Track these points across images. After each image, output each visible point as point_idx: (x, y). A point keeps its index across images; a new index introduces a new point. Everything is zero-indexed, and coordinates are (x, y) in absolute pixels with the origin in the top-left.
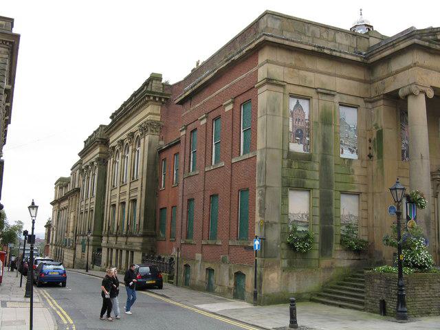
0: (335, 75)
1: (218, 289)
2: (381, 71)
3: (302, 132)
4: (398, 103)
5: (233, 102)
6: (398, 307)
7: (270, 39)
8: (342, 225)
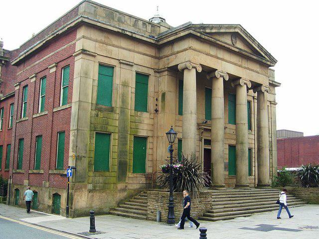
1: (41, 207)
2: (167, 51)
4: (177, 74)
5: (56, 66)
6: (168, 215)
7: (86, 20)
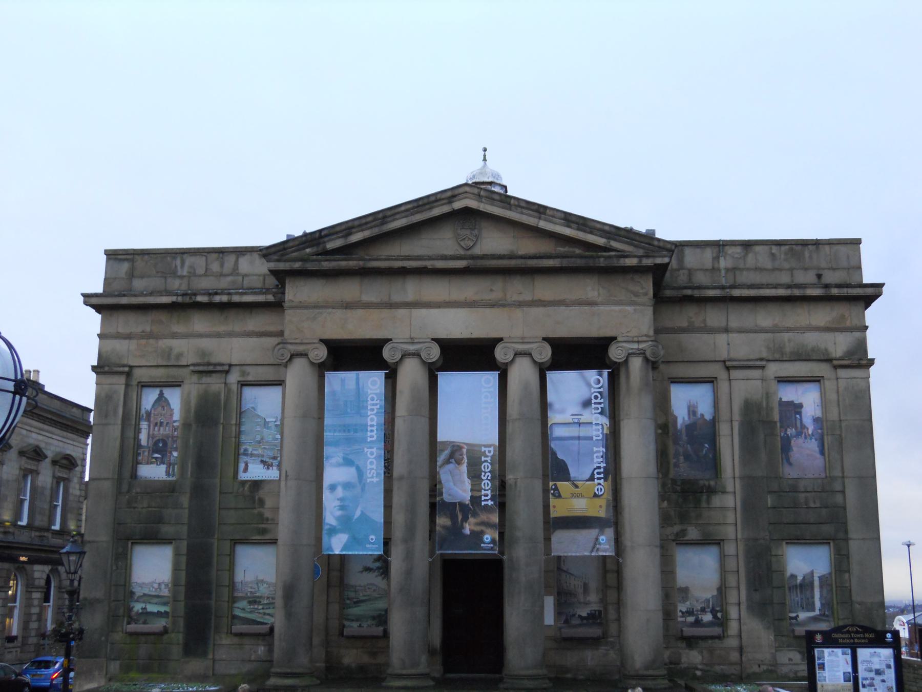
0: (231, 335)
3: (165, 444)
8: (243, 598)
